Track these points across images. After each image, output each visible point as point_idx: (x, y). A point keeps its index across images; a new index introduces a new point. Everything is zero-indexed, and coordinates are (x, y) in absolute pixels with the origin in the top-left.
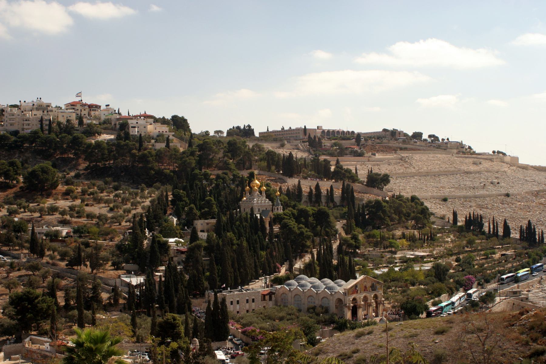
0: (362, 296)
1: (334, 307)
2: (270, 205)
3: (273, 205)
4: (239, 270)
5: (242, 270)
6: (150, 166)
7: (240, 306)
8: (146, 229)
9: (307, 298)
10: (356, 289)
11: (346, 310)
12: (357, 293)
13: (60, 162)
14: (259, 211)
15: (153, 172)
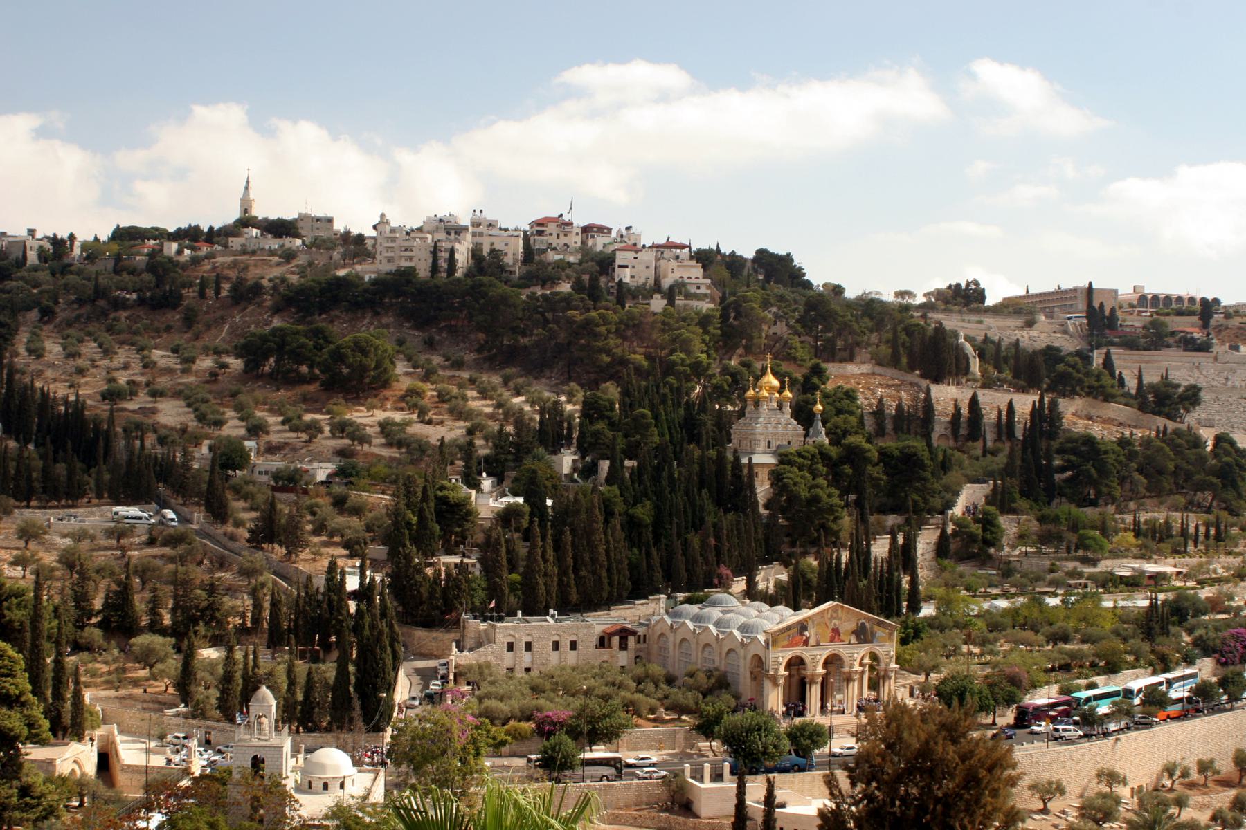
0: (823, 656)
1: (748, 675)
2: (798, 435)
3: (806, 435)
4: (576, 570)
5: (583, 573)
6: (600, 344)
7: (532, 655)
8: (484, 475)
9: (700, 649)
10: (801, 634)
11: (767, 684)
12: (806, 643)
13: (444, 335)
14: (769, 447)
15: (607, 359)
